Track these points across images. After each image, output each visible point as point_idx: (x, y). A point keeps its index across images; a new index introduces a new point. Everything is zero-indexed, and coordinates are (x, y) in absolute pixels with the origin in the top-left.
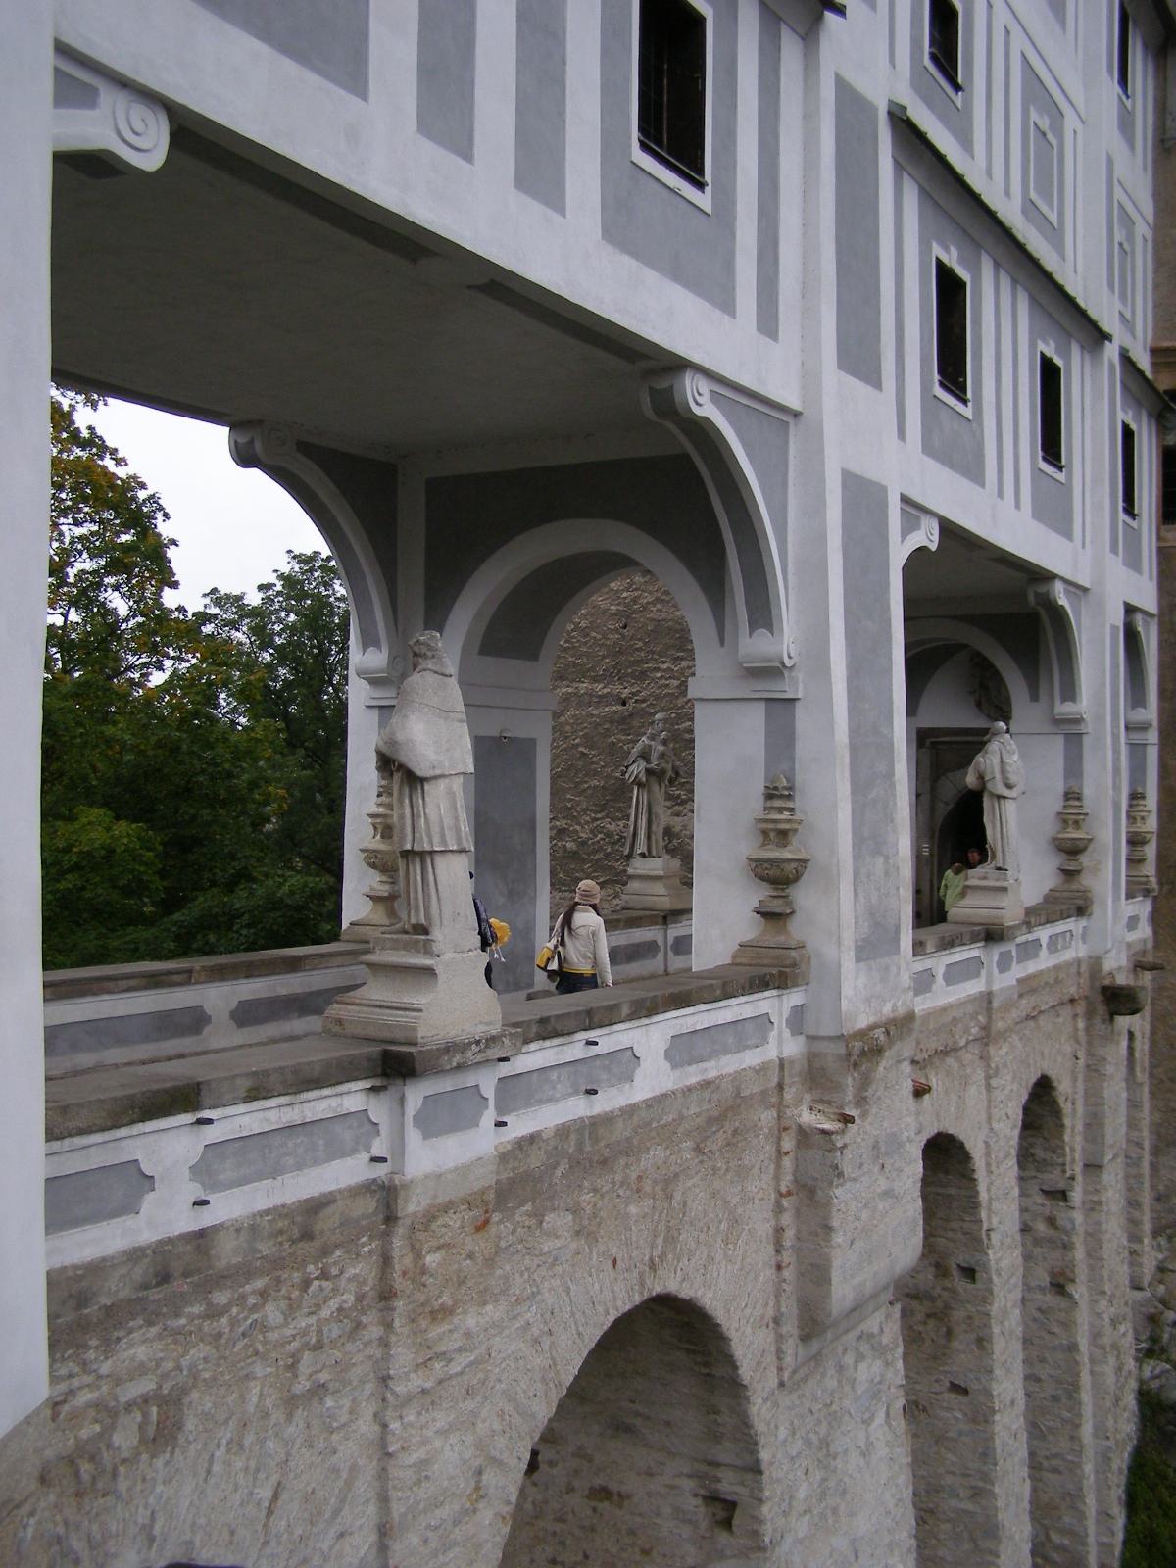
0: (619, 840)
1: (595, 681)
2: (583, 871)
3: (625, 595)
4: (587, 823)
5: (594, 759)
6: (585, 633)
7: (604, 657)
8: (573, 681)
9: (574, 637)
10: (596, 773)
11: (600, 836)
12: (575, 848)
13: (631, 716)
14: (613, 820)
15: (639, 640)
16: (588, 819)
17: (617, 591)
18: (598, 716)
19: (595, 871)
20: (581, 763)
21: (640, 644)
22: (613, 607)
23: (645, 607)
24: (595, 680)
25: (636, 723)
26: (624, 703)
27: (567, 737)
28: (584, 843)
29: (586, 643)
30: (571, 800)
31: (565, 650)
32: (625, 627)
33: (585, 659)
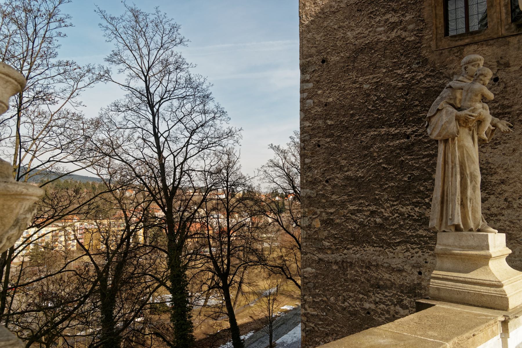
0: (408, 217)
1: (390, 127)
2: (386, 235)
3: (407, 76)
4: (388, 207)
5: (391, 171)
6: (383, 100)
7: (395, 112)
8: (378, 128)
9: (377, 104)
10: (392, 179)
11: (396, 215)
12: (381, 222)
13: (413, 144)
14: (404, 205)
15: (417, 100)
16: (389, 205)
17: (402, 75)
18: (393, 146)
19: (394, 235)
20: (384, 173)
21: (417, 103)
22: (400, 84)
23: (419, 81)
24: (390, 126)
25: (416, 149)
26: (408, 137)
27: (375, 159)
28: (387, 219)
29: (384, 106)
30: (377, 195)
31: (372, 111)
32: (407, 94)
33: (384, 115)
